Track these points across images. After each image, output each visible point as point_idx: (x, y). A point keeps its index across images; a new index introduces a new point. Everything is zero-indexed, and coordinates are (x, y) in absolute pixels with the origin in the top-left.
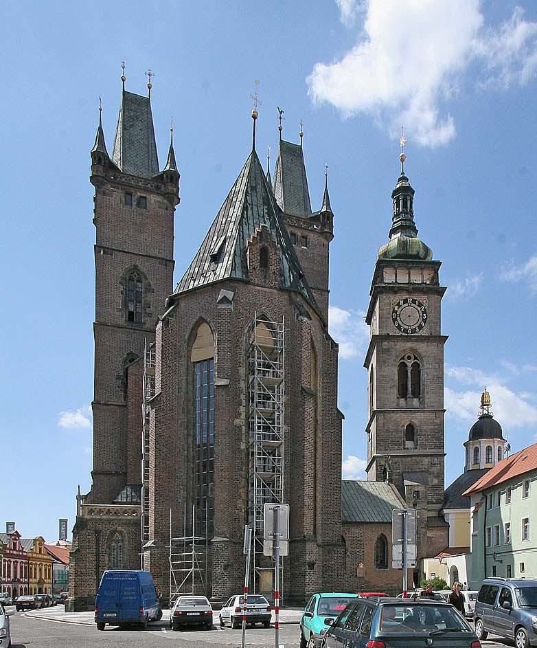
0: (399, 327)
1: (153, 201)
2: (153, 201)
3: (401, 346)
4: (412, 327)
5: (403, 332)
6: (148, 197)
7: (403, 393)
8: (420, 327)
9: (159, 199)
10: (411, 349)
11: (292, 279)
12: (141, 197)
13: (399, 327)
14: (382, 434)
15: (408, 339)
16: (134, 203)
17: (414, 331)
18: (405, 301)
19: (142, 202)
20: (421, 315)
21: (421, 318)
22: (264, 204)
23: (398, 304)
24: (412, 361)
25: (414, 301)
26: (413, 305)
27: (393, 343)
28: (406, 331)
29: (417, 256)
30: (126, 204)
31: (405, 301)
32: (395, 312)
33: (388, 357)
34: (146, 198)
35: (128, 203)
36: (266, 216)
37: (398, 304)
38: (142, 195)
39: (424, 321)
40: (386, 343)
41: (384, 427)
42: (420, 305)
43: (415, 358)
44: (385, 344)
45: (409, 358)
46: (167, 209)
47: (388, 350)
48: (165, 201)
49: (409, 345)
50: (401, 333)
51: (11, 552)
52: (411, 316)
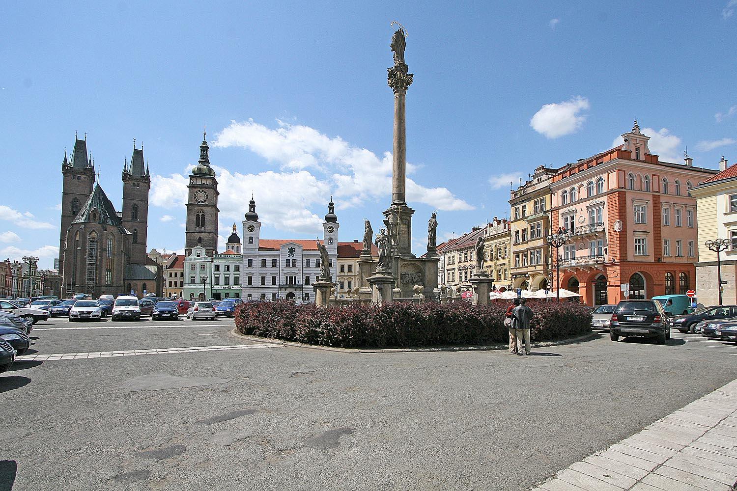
0: (197, 201)
3: (197, 208)
7: (197, 224)
8: (205, 201)
9: (85, 176)
13: (197, 201)
15: (200, 205)
17: (202, 202)
18: (199, 191)
19: (79, 178)
23: (197, 192)
28: (199, 202)
29: (206, 174)
31: (199, 191)
37: (197, 192)
39: (207, 198)
42: (205, 192)
45: (201, 212)
49: (200, 208)
52: (201, 196)
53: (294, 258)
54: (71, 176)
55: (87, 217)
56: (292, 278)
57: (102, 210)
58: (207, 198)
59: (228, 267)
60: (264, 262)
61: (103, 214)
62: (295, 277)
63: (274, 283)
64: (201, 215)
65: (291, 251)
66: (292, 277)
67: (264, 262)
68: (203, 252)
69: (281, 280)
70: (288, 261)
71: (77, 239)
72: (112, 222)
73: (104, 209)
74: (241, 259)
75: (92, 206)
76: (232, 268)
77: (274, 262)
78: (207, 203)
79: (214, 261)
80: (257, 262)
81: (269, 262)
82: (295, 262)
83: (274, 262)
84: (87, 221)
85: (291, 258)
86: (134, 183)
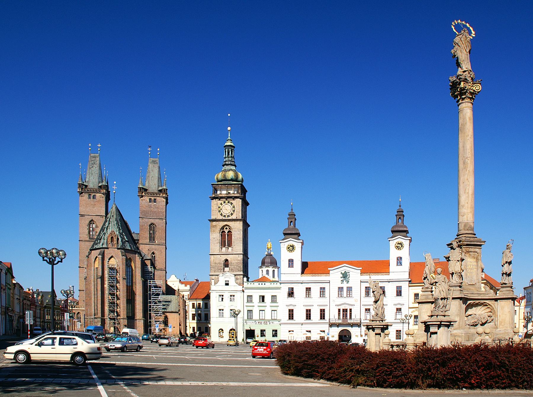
0: (221, 215)
1: (98, 196)
2: (98, 196)
3: (223, 224)
4: (228, 214)
5: (224, 217)
6: (96, 195)
8: (232, 214)
9: (100, 194)
10: (227, 225)
11: (121, 244)
12: (94, 195)
13: (221, 215)
14: (213, 265)
16: (92, 198)
17: (228, 216)
19: (94, 197)
20: (232, 208)
21: (232, 210)
22: (116, 221)
24: (228, 230)
25: (229, 202)
26: (228, 204)
27: (217, 222)
28: (225, 216)
30: (89, 198)
31: (224, 202)
32: (219, 207)
33: (216, 229)
34: (95, 195)
35: (89, 198)
36: (116, 225)
37: (221, 204)
38: (94, 194)
40: (215, 222)
41: (214, 261)
42: (232, 204)
43: (229, 228)
44: (214, 223)
45: (226, 228)
46: (103, 198)
47: (216, 226)
48: (102, 195)
50: (222, 217)
51: (64, 309)
53: (349, 285)
54: (86, 196)
55: (105, 241)
56: (347, 312)
57: (119, 232)
58: (234, 211)
59: (263, 297)
60: (308, 290)
61: (121, 237)
62: (351, 310)
63: (322, 317)
64: (226, 232)
65: (345, 276)
66: (347, 310)
67: (308, 290)
68: (232, 280)
69: (332, 315)
70: (341, 289)
71: (96, 266)
72: (130, 246)
73: (121, 231)
74: (279, 288)
75: (110, 229)
76: (268, 299)
77: (323, 290)
78: (234, 217)
79: (245, 291)
80: (299, 290)
81: (315, 290)
82: (349, 289)
83: (323, 290)
84: (105, 246)
85: (345, 285)
86: (150, 199)
